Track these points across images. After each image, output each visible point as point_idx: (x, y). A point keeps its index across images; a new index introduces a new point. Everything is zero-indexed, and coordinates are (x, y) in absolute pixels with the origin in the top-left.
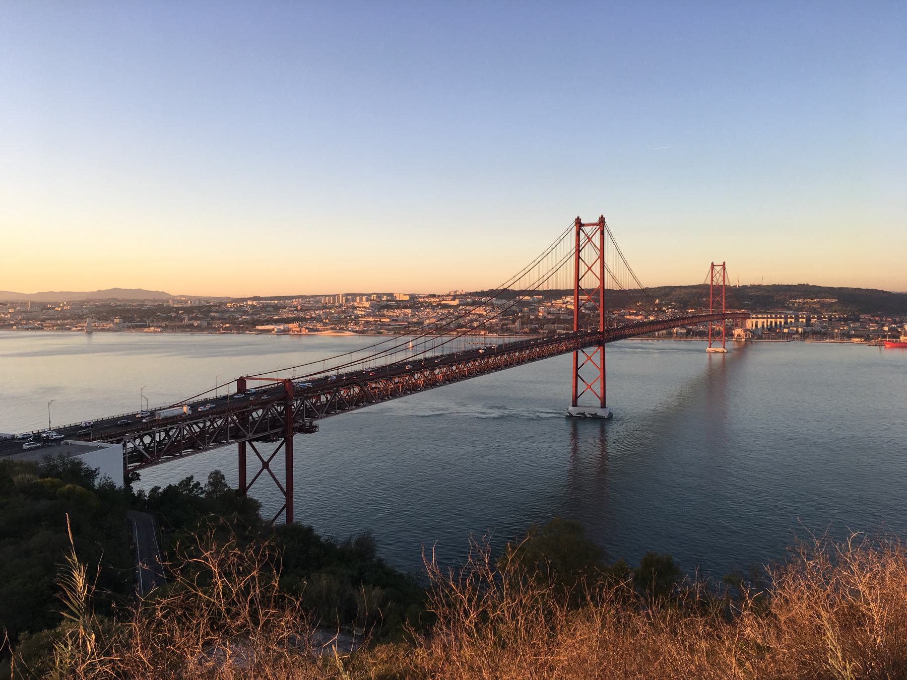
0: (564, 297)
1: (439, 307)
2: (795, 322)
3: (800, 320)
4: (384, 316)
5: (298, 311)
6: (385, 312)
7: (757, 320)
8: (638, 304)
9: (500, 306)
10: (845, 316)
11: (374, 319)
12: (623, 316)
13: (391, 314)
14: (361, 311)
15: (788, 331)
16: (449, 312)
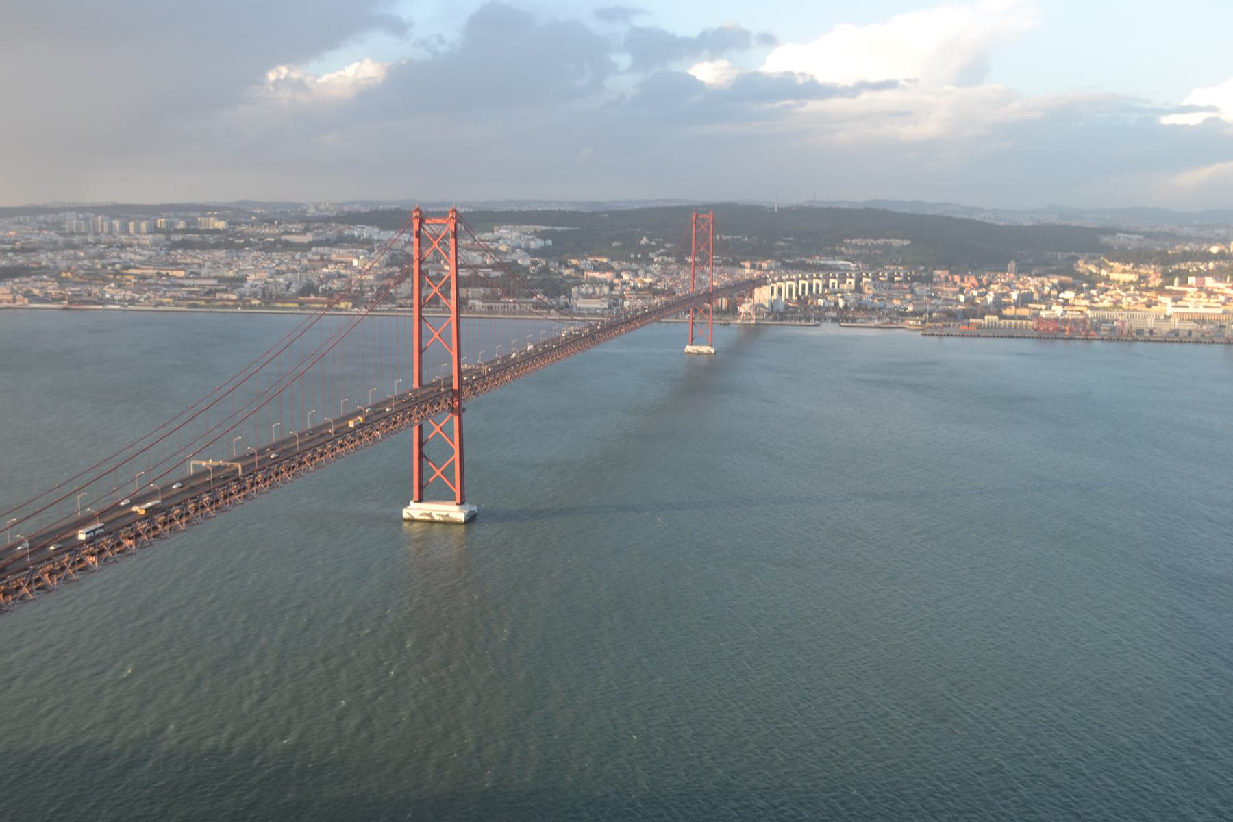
0: (496, 228)
1: (279, 246)
2: (839, 284)
3: (848, 280)
4: (175, 265)
5: (13, 250)
6: (179, 256)
7: (779, 284)
8: (614, 244)
9: (385, 247)
10: (914, 273)
11: (155, 271)
12: (582, 271)
13: (189, 260)
14: (135, 253)
15: (824, 304)
16: (293, 257)
